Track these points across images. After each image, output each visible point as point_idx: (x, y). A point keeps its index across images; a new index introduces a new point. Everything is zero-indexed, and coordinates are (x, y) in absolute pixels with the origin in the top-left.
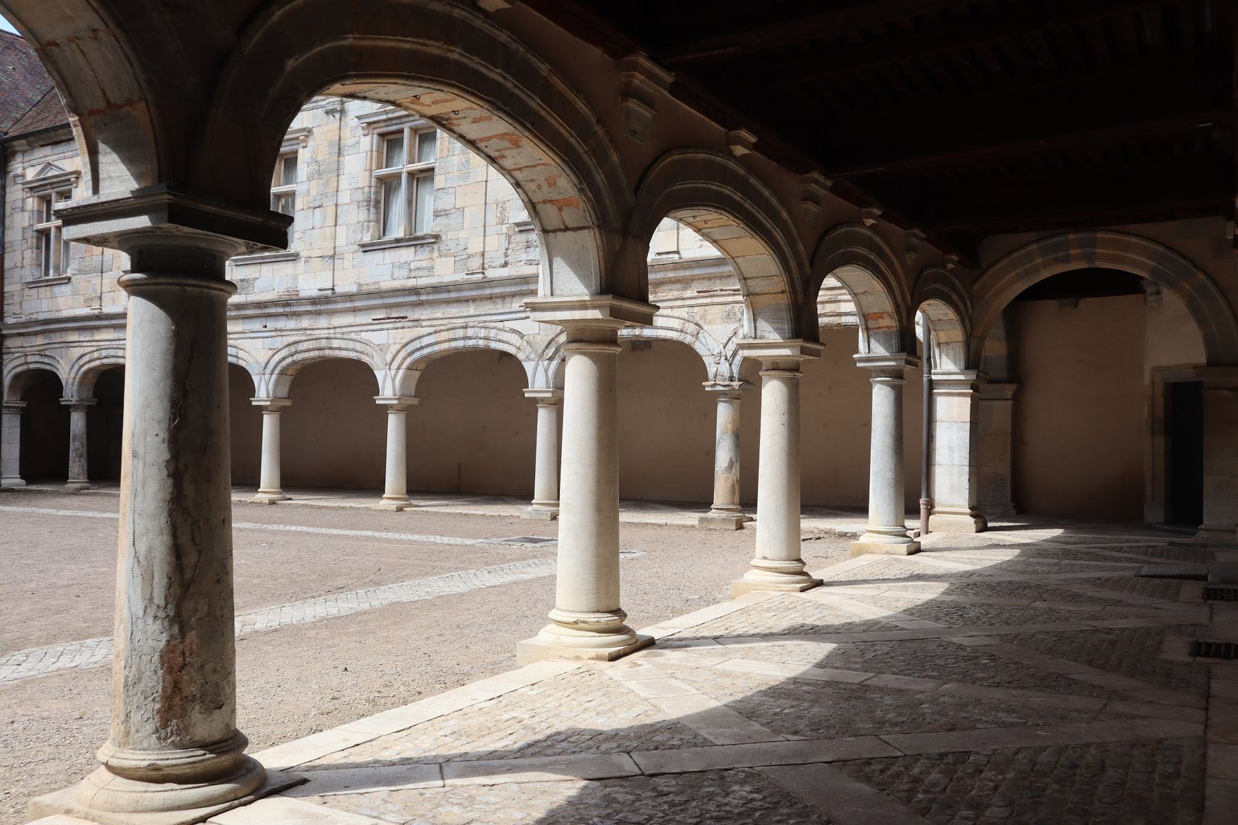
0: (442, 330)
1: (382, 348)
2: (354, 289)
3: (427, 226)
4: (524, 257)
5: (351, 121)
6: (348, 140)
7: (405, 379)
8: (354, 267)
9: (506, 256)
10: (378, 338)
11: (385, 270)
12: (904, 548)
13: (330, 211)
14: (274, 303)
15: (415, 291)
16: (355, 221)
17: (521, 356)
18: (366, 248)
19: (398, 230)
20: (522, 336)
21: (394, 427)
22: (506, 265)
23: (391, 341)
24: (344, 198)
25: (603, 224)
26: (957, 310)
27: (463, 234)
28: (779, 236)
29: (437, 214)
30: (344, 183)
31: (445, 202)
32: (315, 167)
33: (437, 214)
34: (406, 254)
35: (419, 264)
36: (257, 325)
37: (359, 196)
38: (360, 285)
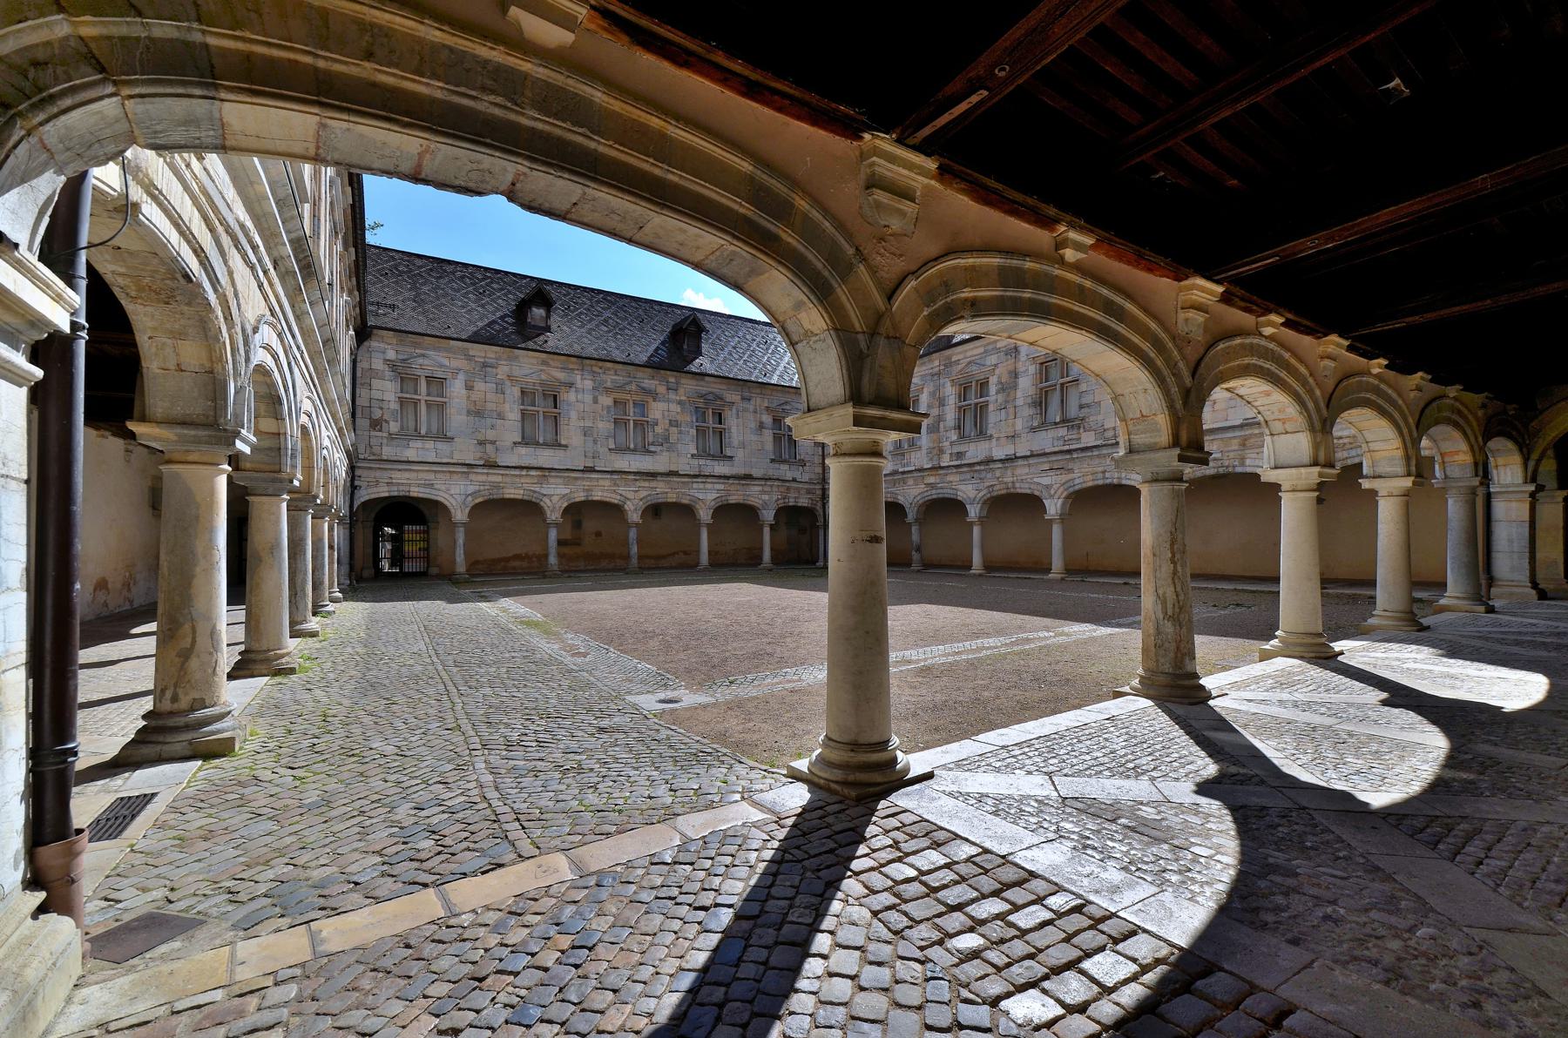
1: (1048, 487)
3: (1073, 411)
5: (1023, 357)
6: (1021, 368)
7: (1063, 504)
11: (1047, 440)
12: (1482, 608)
14: (979, 463)
15: (1069, 452)
16: (1025, 415)
18: (1033, 430)
19: (1055, 414)
21: (1056, 531)
24: (1020, 402)
25: (1312, 429)
26: (1516, 442)
27: (1100, 418)
28: (1396, 415)
29: (1081, 407)
30: (1019, 394)
31: (1087, 400)
33: (1081, 407)
34: (1062, 432)
36: (968, 476)
37: (1029, 400)
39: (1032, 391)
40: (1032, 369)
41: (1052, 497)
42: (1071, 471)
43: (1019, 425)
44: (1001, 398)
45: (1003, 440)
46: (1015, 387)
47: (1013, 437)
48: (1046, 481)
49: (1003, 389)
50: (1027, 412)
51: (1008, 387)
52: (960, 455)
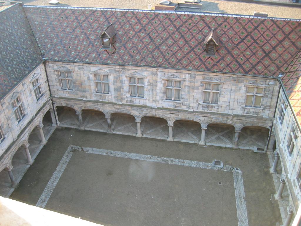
0: (182, 116)
2: (162, 107)
4: (202, 109)
6: (158, 80)
8: (161, 103)
9: (198, 108)
10: (168, 115)
13: (155, 93)
17: (200, 123)
20: (201, 120)
22: (198, 109)
23: (171, 117)
24: (158, 91)
30: (158, 88)
32: (149, 83)
35: (178, 106)
38: (163, 107)
39: (162, 88)
40: (163, 82)
41: (170, 120)
42: (178, 115)
43: (158, 98)
44: (150, 87)
45: (151, 101)
46: (156, 86)
47: (155, 101)
48: (168, 115)
49: (150, 84)
50: (161, 95)
51: (153, 85)
52: (131, 101)
